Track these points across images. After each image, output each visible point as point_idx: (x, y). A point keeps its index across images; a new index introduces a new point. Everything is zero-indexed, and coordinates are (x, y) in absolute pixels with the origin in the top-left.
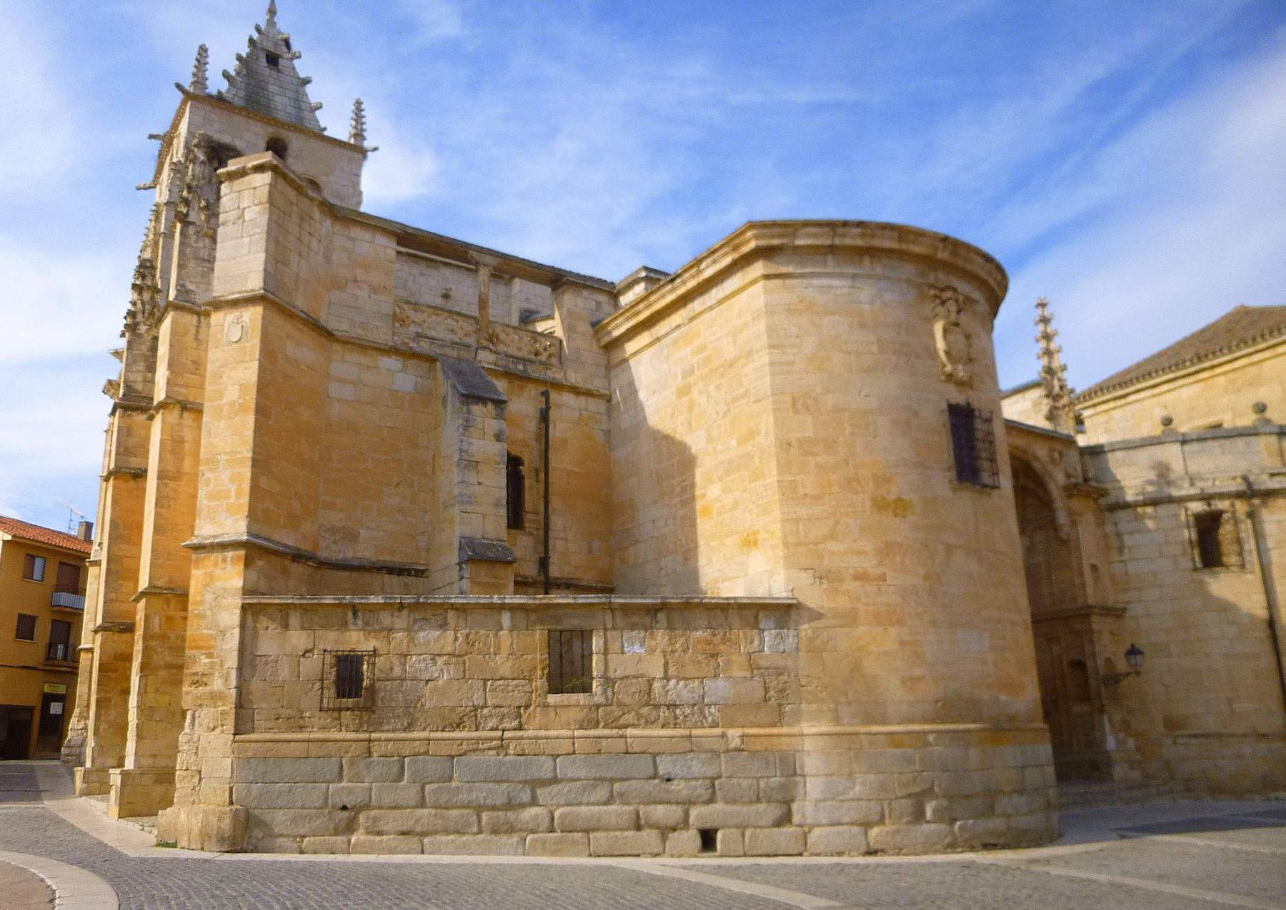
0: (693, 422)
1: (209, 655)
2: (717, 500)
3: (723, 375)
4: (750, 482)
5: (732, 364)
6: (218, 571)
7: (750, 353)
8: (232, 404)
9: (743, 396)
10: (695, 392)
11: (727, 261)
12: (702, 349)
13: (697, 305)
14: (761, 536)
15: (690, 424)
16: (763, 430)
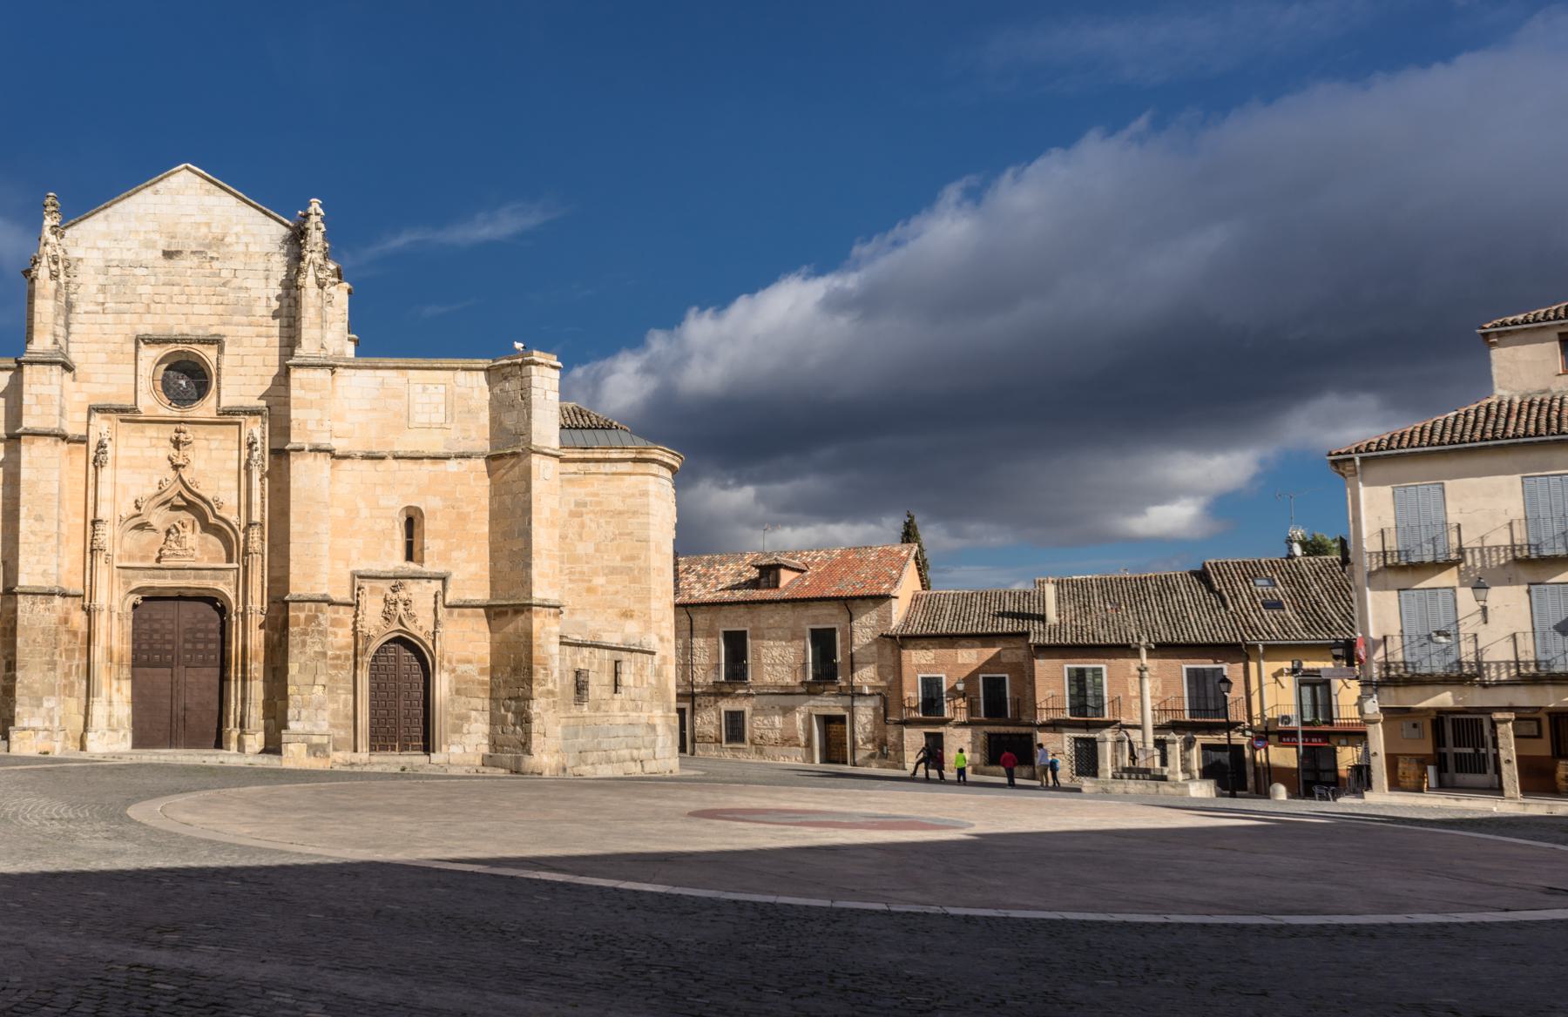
0: (584, 536)
1: (545, 669)
2: (602, 586)
3: (612, 517)
4: (630, 582)
5: (620, 513)
6: (547, 621)
7: (635, 513)
8: (547, 519)
9: (629, 534)
10: (586, 518)
11: (633, 456)
12: (596, 495)
13: (592, 467)
14: (636, 613)
15: (580, 536)
16: (643, 557)
